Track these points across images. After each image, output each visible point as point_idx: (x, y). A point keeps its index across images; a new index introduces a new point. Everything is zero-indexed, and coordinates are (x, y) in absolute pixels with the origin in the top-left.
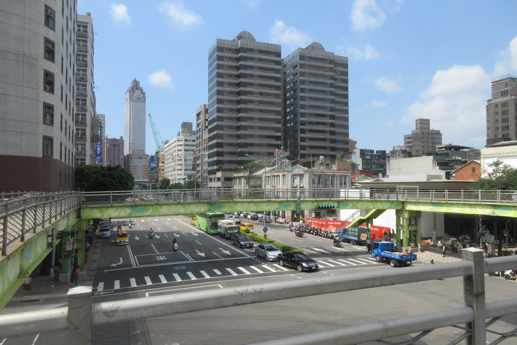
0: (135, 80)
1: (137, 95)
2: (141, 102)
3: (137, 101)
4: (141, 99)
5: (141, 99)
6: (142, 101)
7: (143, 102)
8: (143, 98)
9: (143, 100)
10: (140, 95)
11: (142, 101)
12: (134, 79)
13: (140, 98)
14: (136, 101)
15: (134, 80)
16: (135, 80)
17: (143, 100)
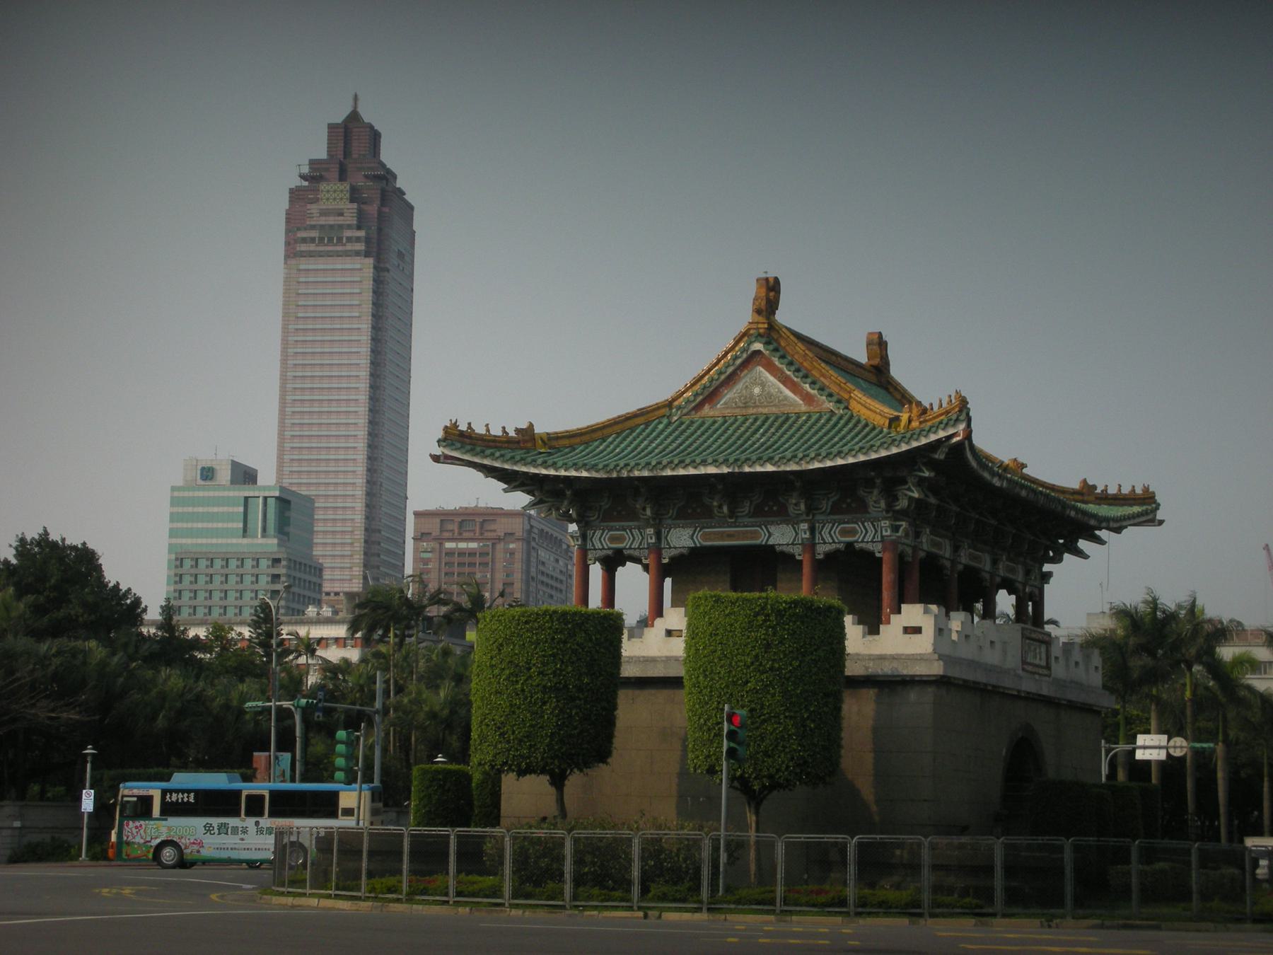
0: (354, 117)
1: (324, 213)
2: (347, 254)
3: (321, 254)
4: (348, 233)
5: (348, 233)
6: (349, 247)
7: (357, 253)
8: (359, 228)
9: (358, 239)
10: (342, 214)
11: (349, 247)
12: (347, 111)
13: (341, 227)
14: (311, 254)
15: (339, 119)
16: (354, 117)
17: (358, 239)
